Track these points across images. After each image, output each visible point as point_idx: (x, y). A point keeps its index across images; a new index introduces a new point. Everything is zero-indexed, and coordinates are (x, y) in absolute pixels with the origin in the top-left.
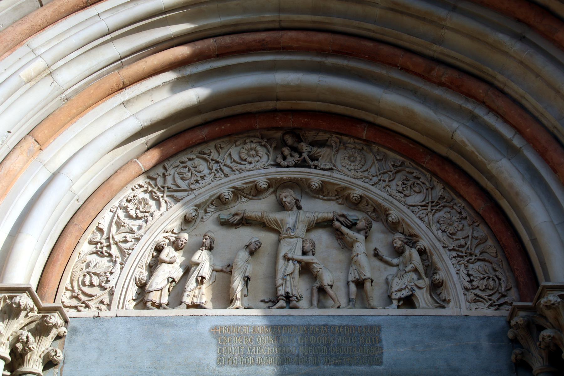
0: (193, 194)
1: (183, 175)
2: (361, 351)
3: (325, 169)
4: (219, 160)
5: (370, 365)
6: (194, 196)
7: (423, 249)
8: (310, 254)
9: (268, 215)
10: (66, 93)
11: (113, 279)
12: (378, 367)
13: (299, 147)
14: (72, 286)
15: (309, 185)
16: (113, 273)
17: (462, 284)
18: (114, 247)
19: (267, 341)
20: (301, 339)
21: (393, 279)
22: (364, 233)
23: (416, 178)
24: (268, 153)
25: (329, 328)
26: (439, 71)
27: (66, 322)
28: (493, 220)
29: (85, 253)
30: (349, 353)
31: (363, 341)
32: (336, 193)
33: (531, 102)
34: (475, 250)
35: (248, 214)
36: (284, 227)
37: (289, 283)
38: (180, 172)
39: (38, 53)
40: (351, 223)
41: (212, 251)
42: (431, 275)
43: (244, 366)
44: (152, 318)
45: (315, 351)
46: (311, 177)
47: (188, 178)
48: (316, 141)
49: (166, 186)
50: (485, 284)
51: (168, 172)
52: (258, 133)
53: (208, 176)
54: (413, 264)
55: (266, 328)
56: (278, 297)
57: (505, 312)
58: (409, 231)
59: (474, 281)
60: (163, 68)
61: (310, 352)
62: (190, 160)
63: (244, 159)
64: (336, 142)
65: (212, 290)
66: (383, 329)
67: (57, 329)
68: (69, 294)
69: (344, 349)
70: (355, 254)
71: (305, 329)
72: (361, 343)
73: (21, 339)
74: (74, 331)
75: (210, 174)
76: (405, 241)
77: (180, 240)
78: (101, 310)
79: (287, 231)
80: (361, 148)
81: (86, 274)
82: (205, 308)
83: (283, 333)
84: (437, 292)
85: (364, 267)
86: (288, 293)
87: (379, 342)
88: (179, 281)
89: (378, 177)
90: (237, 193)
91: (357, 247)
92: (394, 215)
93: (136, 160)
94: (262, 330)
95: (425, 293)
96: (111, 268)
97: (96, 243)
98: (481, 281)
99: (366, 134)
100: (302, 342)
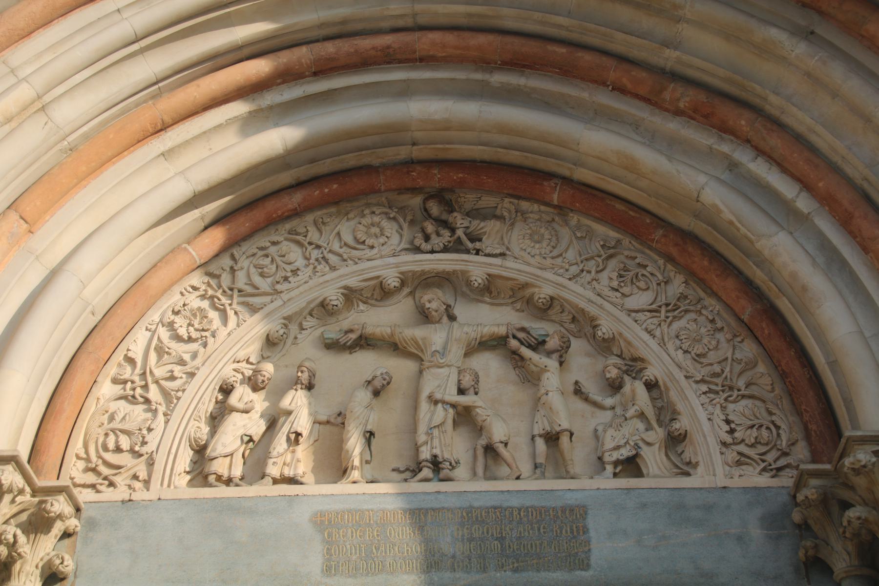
0: (280, 300)
1: (262, 268)
2: (555, 547)
3: (492, 254)
4: (320, 243)
5: (571, 570)
6: (282, 303)
8: (470, 393)
9: (401, 331)
10: (70, 139)
11: (153, 440)
12: (583, 573)
13: (451, 219)
14: (87, 452)
15: (467, 281)
16: (153, 429)
18: (153, 387)
19: (403, 535)
20: (458, 529)
21: (605, 431)
23: (640, 265)
24: (401, 231)
25: (503, 511)
26: (672, 92)
27: (78, 510)
28: (766, 332)
29: (107, 397)
30: (536, 550)
31: (559, 531)
32: (512, 294)
33: (823, 139)
34: (737, 381)
35: (369, 330)
36: (428, 350)
37: (437, 440)
38: (257, 265)
39: (22, 74)
40: (536, 342)
41: (312, 391)
42: (667, 422)
43: (367, 575)
44: (217, 501)
45: (481, 549)
47: (272, 274)
49: (236, 288)
50: (754, 436)
51: (239, 265)
52: (383, 199)
53: (303, 269)
54: (637, 405)
55: (401, 513)
56: (420, 463)
57: (787, 480)
58: (629, 351)
59: (736, 430)
60: (226, 95)
61: (472, 551)
62: (274, 243)
63: (361, 241)
65: (314, 453)
66: (589, 512)
67: (63, 521)
68: (81, 465)
69: (527, 545)
71: (465, 514)
72: (555, 534)
73: (5, 539)
74: (91, 524)
75: (307, 266)
76: (624, 368)
77: (261, 375)
78: (134, 490)
79: (432, 357)
81: (109, 431)
82: (302, 484)
83: (430, 521)
84: (677, 449)
85: (558, 413)
86: (435, 456)
87: (584, 533)
88: (260, 441)
89: (579, 266)
90: (351, 296)
91: (546, 379)
92: (606, 328)
93: (186, 245)
94: (394, 517)
95: (657, 452)
96: (149, 422)
97: (125, 382)
98: (749, 431)
99: (558, 197)
100: (460, 534)
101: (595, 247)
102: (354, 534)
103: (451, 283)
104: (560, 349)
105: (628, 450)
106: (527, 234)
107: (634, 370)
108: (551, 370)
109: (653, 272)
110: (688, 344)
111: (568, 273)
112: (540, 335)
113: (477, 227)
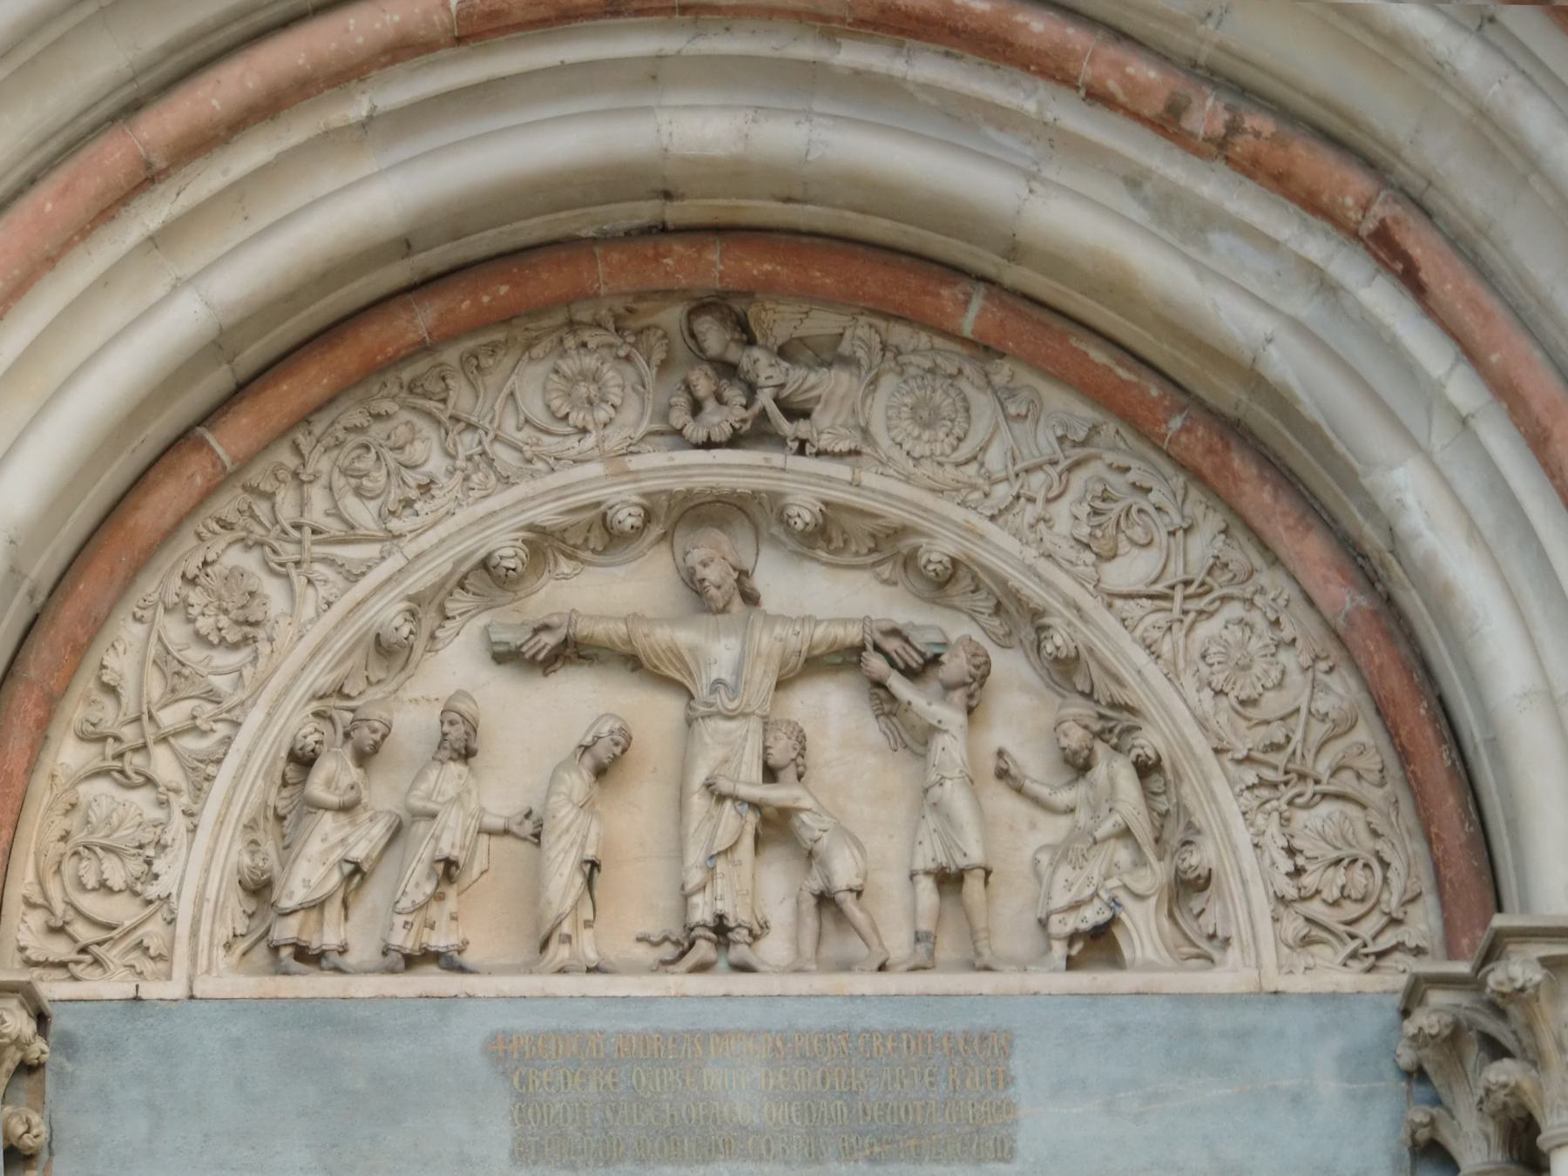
0: (399, 555)
6: (403, 562)
7: (1149, 758)
12: (1002, 1167)
13: (745, 364)
14: (46, 897)
15: (782, 513)
17: (1267, 882)
20: (767, 1075)
21: (1054, 865)
22: (964, 697)
27: (41, 1019)
32: (872, 545)
35: (583, 629)
36: (704, 676)
41: (471, 760)
45: (810, 1114)
46: (786, 486)
48: (800, 339)
49: (308, 525)
52: (603, 312)
56: (692, 929)
57: (1394, 977)
59: (1305, 871)
61: (794, 1119)
62: (377, 417)
64: (870, 348)
66: (1018, 1042)
69: (899, 1108)
70: (934, 777)
72: (951, 1088)
76: (1097, 726)
80: (955, 371)
81: (81, 849)
86: (721, 917)
89: (1011, 486)
91: (940, 748)
97: (102, 739)
98: (1331, 871)
101: (1046, 441)
102: (570, 1081)
103: (748, 516)
104: (969, 680)
105: (1097, 909)
106: (906, 405)
107: (1115, 726)
108: (954, 729)
109: (1161, 505)
110: (1222, 677)
111: (989, 502)
112: (928, 644)
113: (799, 387)
